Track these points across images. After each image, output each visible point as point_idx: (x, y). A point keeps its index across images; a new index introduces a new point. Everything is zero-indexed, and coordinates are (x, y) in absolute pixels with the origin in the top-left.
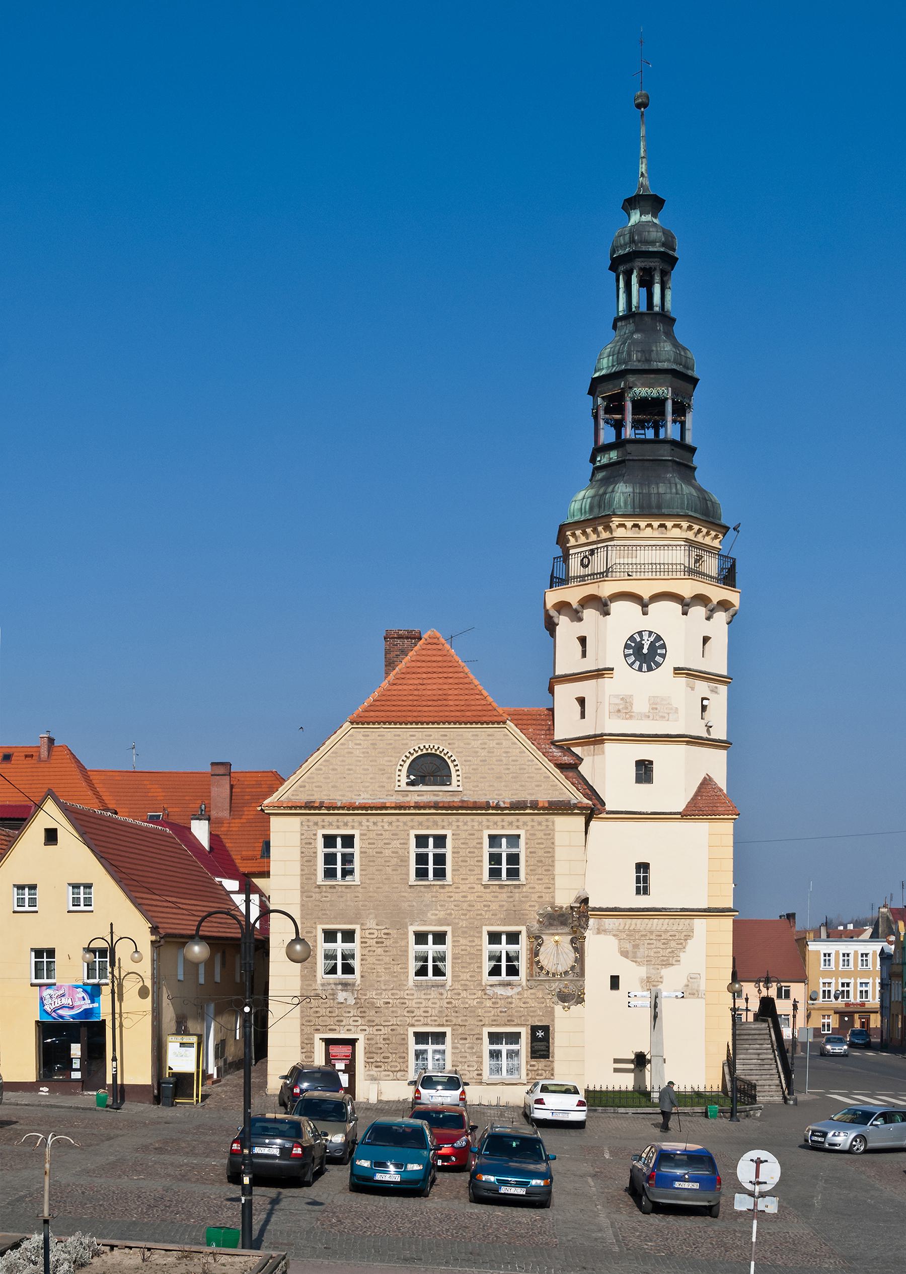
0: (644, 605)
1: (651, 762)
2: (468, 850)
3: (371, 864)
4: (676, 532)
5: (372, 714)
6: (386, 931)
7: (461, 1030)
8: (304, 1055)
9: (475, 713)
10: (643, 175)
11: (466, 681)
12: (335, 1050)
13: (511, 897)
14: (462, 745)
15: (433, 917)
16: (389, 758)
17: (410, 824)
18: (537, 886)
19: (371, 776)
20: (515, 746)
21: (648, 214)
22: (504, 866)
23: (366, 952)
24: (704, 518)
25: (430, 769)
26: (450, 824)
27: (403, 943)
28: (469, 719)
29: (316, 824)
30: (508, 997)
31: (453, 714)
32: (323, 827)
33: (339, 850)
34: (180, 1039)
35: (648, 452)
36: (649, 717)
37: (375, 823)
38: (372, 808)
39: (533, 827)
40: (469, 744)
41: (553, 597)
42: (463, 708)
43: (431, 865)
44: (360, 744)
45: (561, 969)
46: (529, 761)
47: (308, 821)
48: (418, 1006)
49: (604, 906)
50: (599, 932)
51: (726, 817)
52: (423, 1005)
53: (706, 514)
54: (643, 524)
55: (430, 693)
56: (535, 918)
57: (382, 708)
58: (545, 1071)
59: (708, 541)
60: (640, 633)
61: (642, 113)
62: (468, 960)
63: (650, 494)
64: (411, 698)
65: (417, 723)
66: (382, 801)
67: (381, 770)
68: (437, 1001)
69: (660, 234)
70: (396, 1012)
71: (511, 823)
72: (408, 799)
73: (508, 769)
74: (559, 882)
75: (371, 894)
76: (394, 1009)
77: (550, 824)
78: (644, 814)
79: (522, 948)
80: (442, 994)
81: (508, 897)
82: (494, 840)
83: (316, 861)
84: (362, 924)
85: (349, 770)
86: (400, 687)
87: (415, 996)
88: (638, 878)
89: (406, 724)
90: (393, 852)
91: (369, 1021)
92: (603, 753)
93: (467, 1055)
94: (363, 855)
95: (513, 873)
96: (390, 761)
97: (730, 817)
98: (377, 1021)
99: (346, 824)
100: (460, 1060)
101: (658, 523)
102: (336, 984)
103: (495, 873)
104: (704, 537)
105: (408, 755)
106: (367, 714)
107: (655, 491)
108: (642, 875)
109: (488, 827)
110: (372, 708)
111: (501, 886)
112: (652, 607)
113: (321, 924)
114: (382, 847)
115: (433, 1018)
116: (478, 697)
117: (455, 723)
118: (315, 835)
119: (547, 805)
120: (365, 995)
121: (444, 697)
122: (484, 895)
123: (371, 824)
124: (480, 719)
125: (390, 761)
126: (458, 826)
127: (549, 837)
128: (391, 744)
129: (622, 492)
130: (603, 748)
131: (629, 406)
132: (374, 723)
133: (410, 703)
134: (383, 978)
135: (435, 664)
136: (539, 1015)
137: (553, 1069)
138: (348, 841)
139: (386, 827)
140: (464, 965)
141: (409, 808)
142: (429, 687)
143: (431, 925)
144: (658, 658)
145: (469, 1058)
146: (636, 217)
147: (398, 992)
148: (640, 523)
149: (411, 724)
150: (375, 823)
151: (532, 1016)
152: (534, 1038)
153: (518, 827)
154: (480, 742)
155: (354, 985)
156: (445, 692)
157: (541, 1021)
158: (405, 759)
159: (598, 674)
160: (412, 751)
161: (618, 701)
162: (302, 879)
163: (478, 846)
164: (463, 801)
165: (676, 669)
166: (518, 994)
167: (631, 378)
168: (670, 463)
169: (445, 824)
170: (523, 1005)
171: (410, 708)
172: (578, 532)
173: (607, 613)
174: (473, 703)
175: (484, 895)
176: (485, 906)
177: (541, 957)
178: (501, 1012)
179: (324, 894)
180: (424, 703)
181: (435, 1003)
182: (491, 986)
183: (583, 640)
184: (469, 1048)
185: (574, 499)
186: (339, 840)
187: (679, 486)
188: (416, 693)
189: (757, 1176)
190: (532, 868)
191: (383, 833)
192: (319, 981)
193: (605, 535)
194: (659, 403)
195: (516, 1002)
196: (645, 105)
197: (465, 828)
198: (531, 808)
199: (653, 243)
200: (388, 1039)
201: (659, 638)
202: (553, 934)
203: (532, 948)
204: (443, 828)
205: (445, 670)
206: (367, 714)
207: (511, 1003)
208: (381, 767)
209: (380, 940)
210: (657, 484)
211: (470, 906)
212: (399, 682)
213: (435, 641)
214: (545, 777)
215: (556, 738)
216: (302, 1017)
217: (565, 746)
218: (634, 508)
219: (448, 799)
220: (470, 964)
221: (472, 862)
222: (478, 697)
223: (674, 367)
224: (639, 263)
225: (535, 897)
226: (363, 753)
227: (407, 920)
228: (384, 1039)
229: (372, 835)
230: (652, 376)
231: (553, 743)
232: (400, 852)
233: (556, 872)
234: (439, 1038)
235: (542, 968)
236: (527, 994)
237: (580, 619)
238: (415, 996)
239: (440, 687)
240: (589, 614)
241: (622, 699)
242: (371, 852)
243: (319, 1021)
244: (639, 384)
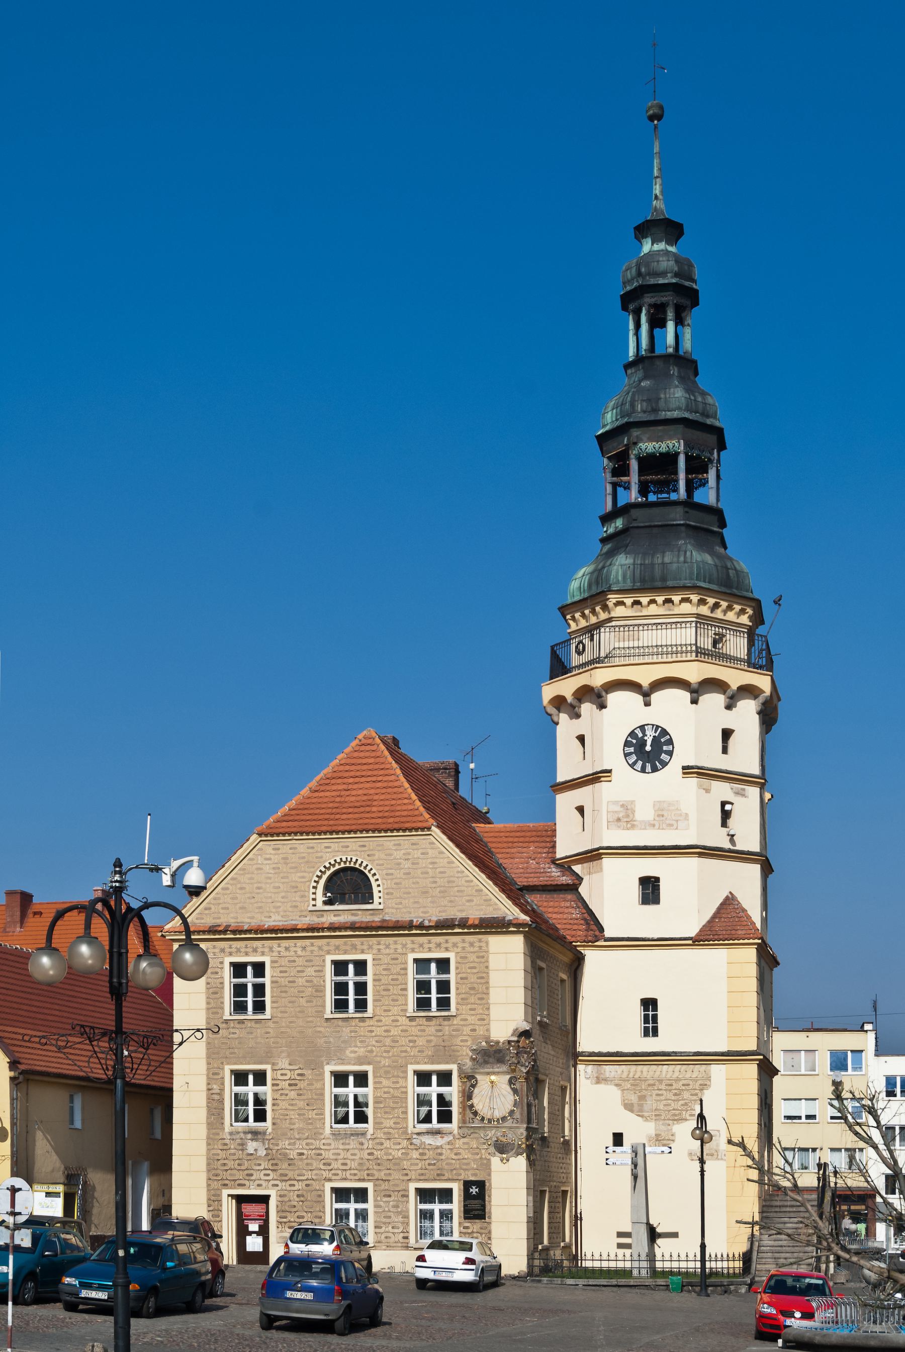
0: (646, 695)
1: (657, 879)
2: (391, 977)
3: (283, 995)
4: (686, 608)
5: (284, 824)
6: (300, 1072)
7: (385, 1186)
8: (211, 1214)
9: (398, 819)
10: (658, 200)
11: (396, 784)
12: (248, 1208)
13: (440, 1031)
14: (383, 856)
15: (353, 1055)
16: (302, 874)
17: (326, 948)
18: (469, 1018)
19: (283, 894)
20: (442, 856)
21: (661, 241)
22: (434, 994)
23: (277, 1096)
24: (723, 589)
25: (348, 884)
26: (370, 947)
27: (318, 1085)
28: (389, 826)
29: (223, 950)
30: (437, 1148)
31: (373, 821)
32: (231, 954)
33: (250, 979)
34: (45, 1188)
35: (658, 516)
36: (654, 826)
37: (287, 949)
38: (282, 931)
39: (464, 948)
40: (391, 855)
41: (549, 691)
42: (386, 814)
43: (350, 995)
44: (270, 859)
45: (498, 1114)
46: (458, 872)
47: (214, 947)
48: (334, 1157)
49: (605, 1051)
51: (746, 941)
52: (341, 1157)
53: (729, 586)
54: (645, 600)
55: (353, 799)
56: (467, 1054)
57: (297, 818)
58: (481, 1234)
59: (731, 616)
60: (642, 728)
61: (656, 127)
62: (391, 1105)
63: (653, 564)
64: (331, 805)
65: (331, 833)
66: (294, 922)
67: (293, 887)
68: (356, 1151)
69: (672, 263)
70: (311, 1164)
71: (439, 945)
72: (323, 920)
73: (436, 882)
74: (494, 1012)
75: (283, 1030)
76: (309, 1161)
77: (483, 944)
78: (649, 940)
79: (453, 1092)
80: (362, 1144)
81: (437, 1031)
82: (422, 964)
83: (223, 993)
84: (273, 1064)
85: (259, 888)
86: (322, 794)
87: (332, 1146)
88: (646, 1018)
89: (319, 834)
90: (307, 981)
91: (281, 1175)
92: (601, 870)
93: (392, 1214)
94: (274, 985)
95: (444, 1004)
96: (303, 877)
97: (751, 941)
98: (290, 1174)
99: (255, 950)
100: (384, 1220)
101: (663, 598)
102: (245, 1133)
103: (423, 1004)
104: (725, 612)
105: (323, 870)
106: (278, 825)
107: (660, 561)
108: (651, 1013)
109: (413, 951)
110: (286, 818)
111: (429, 1018)
112: (654, 697)
113: (228, 1064)
114: (300, 974)
115: (352, 1172)
116: (406, 801)
117: (374, 832)
118: (222, 963)
119: (477, 922)
120: (277, 1145)
121: (369, 803)
122: (409, 1029)
123: (282, 949)
124: (401, 825)
125: (303, 877)
126: (379, 950)
127: (483, 960)
128: (304, 858)
129: (622, 564)
130: (601, 864)
131: (634, 465)
132: (284, 835)
133: (329, 811)
134: (297, 1126)
135: (365, 767)
136: (473, 1169)
137: (490, 1232)
138: (259, 969)
139: (299, 953)
140: (387, 1110)
141: (323, 929)
142: (354, 793)
143: (350, 1064)
144: (664, 757)
145: (394, 1218)
146: (647, 246)
147: (313, 1141)
148: (641, 599)
149: (325, 833)
150: (287, 949)
151: (465, 1170)
152: (467, 1196)
153: (447, 949)
154: (403, 852)
155: (265, 1133)
156: (370, 797)
157: (476, 1175)
158: (319, 874)
159: (594, 778)
160: (328, 865)
161: (618, 808)
162: (207, 1014)
163: (402, 972)
164: (384, 921)
165: (684, 768)
166: (449, 1143)
167: (635, 433)
168: (683, 528)
169: (365, 947)
170: (454, 1157)
171: (327, 816)
172: (577, 615)
173: (602, 706)
174: (399, 808)
175: (409, 1029)
176: (410, 1041)
177: (475, 1101)
178: (429, 1164)
179: (232, 1030)
180: (344, 810)
181: (355, 1155)
182: (418, 1134)
183: (581, 739)
184: (394, 1207)
185: (574, 577)
186: (249, 969)
187: (688, 553)
188: (338, 799)
189: (13, 1205)
190: (463, 996)
191: (297, 959)
192: (227, 1128)
193: (603, 616)
194: (670, 459)
195: (446, 1153)
196: (659, 117)
197: (387, 951)
198: (459, 926)
199: (663, 274)
200: (303, 1196)
201: (664, 732)
202: (488, 1074)
203: (464, 1090)
204: (363, 952)
205: (375, 773)
206: (278, 825)
207: (441, 1154)
208: (293, 884)
209: (293, 1082)
210: (664, 552)
211: (393, 1041)
212: (322, 788)
213: (369, 741)
214: (476, 891)
215: (558, 856)
216: (208, 1171)
217: (565, 866)
218: (634, 582)
219: (367, 918)
220: (393, 1108)
221: (395, 990)
222: (406, 801)
223: (687, 415)
224: (649, 299)
225: (467, 1030)
226: (274, 868)
227: (323, 1059)
228: (298, 1196)
229: (284, 962)
230: (660, 428)
231: (554, 861)
232: (315, 980)
233: (491, 1001)
234: (361, 1195)
235: (476, 1113)
236: (459, 1143)
237: (578, 716)
238: (332, 1146)
239: (366, 792)
240: (587, 708)
241: (622, 806)
242: (283, 981)
243: (227, 1175)
244: (645, 439)
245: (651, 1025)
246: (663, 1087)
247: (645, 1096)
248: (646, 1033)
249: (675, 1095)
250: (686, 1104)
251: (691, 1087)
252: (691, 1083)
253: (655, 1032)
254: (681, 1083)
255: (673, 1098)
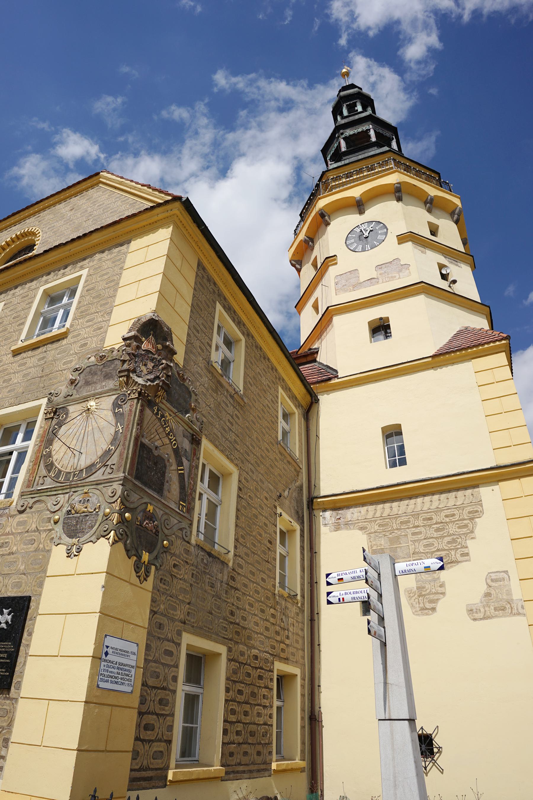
50: (337, 527)
177: (56, 445)
202: (86, 399)
245: (397, 458)
246: (420, 522)
247: (398, 538)
248: (393, 465)
249: (438, 530)
250: (454, 541)
251: (457, 517)
252: (456, 512)
253: (403, 462)
254: (443, 514)
255: (435, 535)
